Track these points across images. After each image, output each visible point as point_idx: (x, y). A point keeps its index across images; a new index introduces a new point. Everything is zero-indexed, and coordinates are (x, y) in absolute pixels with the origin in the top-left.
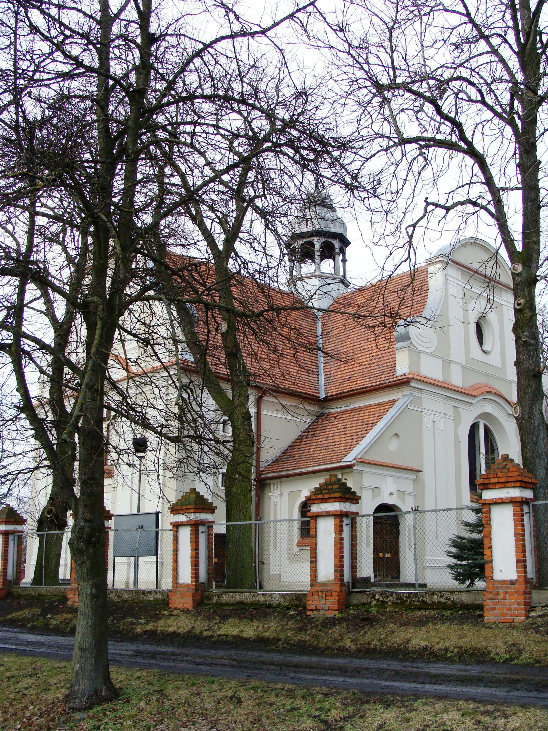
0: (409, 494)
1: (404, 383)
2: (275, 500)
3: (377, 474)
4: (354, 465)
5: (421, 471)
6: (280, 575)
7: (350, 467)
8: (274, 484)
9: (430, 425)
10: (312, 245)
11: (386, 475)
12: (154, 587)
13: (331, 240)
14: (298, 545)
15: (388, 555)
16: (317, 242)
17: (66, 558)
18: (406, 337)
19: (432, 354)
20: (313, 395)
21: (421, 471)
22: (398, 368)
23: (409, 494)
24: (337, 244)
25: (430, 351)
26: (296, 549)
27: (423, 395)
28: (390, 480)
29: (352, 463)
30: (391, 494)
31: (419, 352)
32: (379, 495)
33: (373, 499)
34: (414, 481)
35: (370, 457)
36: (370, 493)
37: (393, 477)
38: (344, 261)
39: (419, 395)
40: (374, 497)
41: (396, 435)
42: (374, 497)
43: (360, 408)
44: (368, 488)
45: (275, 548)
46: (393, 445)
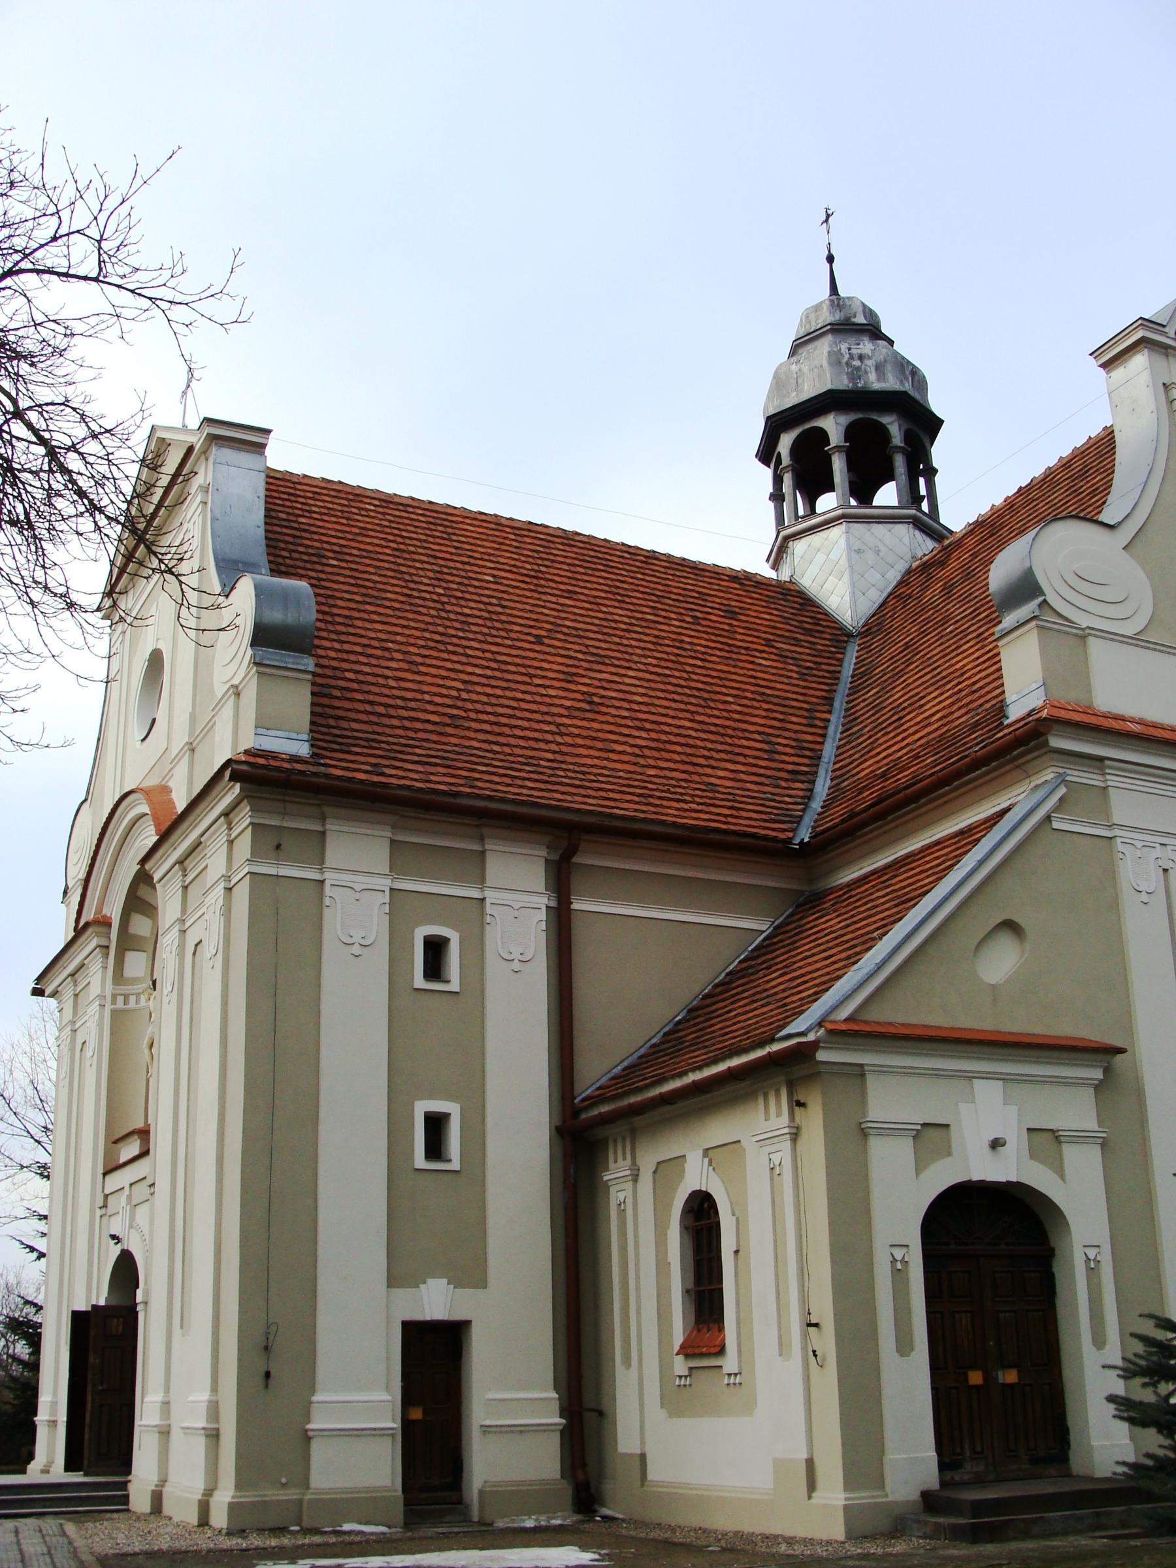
0: (1080, 1138)
1: (1029, 741)
2: (621, 1196)
3: (936, 1074)
4: (815, 1046)
5: (1121, 1051)
6: (643, 1457)
7: (802, 1054)
8: (615, 1141)
9: (1154, 881)
10: (821, 436)
11: (970, 1077)
12: (193, 1519)
13: (875, 417)
14: (688, 1350)
15: (1010, 1377)
16: (833, 426)
17: (54, 1404)
18: (1026, 588)
19: (1136, 641)
20: (765, 838)
21: (1121, 1051)
22: (1010, 697)
23: (1080, 1138)
24: (895, 428)
25: (1129, 629)
26: (680, 1365)
27: (1112, 780)
28: (988, 1093)
29: (811, 1037)
30: (996, 1144)
31: (1083, 636)
32: (946, 1151)
33: (917, 1175)
34: (1097, 1088)
35: (898, 1012)
36: (904, 1148)
37: (1005, 1078)
38: (931, 472)
39: (1093, 779)
40: (920, 1166)
41: (1010, 926)
42: (920, 1166)
43: (908, 856)
44: (891, 1130)
45: (627, 1363)
46: (1001, 963)
